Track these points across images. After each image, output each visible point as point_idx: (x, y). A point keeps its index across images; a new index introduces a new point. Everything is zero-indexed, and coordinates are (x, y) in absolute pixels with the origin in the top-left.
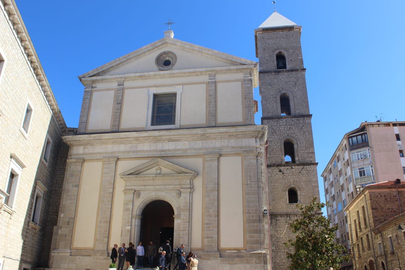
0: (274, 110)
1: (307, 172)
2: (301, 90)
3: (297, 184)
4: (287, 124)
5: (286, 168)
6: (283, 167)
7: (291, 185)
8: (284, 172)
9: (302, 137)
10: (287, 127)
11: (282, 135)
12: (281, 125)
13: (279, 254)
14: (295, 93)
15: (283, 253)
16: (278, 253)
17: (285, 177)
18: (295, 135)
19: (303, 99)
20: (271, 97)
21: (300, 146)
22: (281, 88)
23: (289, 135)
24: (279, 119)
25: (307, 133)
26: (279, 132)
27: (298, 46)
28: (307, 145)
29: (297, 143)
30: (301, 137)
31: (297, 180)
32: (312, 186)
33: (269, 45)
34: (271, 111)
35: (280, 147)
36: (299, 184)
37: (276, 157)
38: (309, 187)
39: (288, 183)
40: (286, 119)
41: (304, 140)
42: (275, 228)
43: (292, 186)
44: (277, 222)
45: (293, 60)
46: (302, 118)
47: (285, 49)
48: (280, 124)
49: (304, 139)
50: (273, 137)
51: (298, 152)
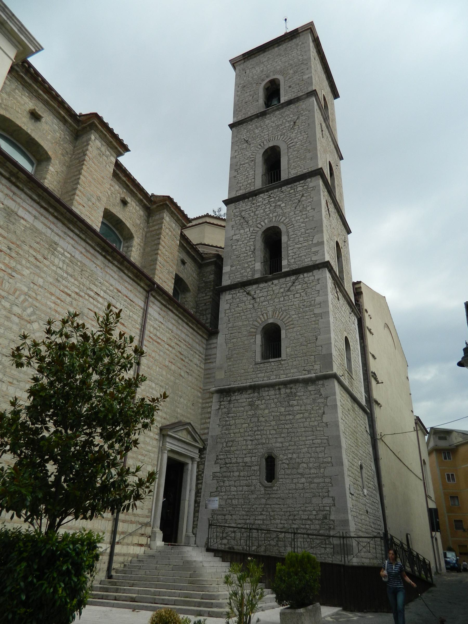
0: (250, 181)
1: (305, 285)
2: (305, 132)
3: (282, 315)
4: (270, 200)
5: (262, 285)
6: (254, 287)
7: (268, 319)
8: (255, 296)
9: (299, 218)
10: (271, 206)
11: (260, 223)
12: (259, 206)
13: (227, 483)
14: (292, 140)
15: (235, 481)
16: (224, 482)
17: (256, 305)
18: (284, 218)
19: (306, 146)
20: (247, 161)
21: (293, 236)
22: (266, 140)
23: (274, 220)
24: (256, 195)
25: (308, 208)
26: (254, 220)
27: (305, 57)
28: (307, 232)
29: (288, 232)
30: (297, 219)
31: (282, 306)
32: (314, 314)
33: (252, 78)
34: (243, 185)
35: (252, 247)
36: (285, 314)
37: (244, 268)
38: (307, 317)
39: (261, 316)
40: (270, 192)
41: (302, 223)
42: (226, 421)
43: (270, 321)
44: (232, 405)
45: (292, 86)
46: (301, 182)
47: (282, 72)
48: (258, 204)
49: (302, 220)
50: (242, 231)
51: (290, 248)
